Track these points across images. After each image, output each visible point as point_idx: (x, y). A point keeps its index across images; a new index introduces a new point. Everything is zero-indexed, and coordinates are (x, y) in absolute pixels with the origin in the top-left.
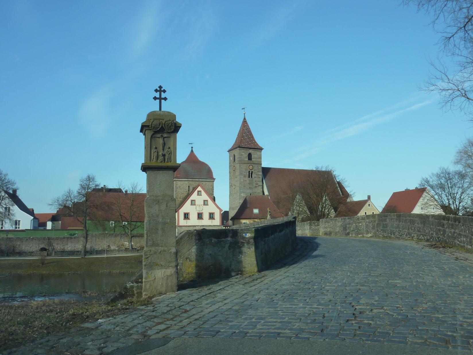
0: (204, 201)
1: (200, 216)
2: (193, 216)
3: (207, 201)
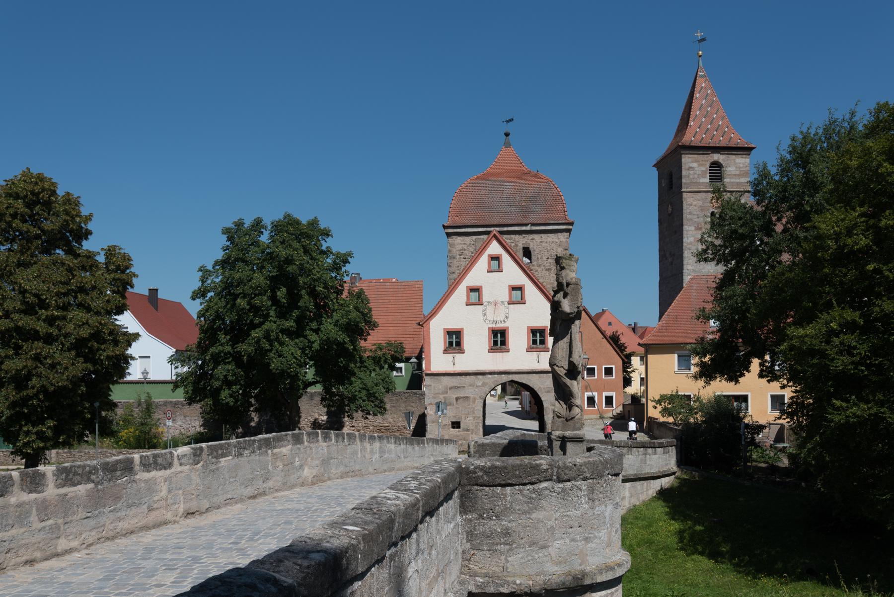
0: (514, 288)
1: (499, 339)
2: (476, 343)
3: (520, 288)
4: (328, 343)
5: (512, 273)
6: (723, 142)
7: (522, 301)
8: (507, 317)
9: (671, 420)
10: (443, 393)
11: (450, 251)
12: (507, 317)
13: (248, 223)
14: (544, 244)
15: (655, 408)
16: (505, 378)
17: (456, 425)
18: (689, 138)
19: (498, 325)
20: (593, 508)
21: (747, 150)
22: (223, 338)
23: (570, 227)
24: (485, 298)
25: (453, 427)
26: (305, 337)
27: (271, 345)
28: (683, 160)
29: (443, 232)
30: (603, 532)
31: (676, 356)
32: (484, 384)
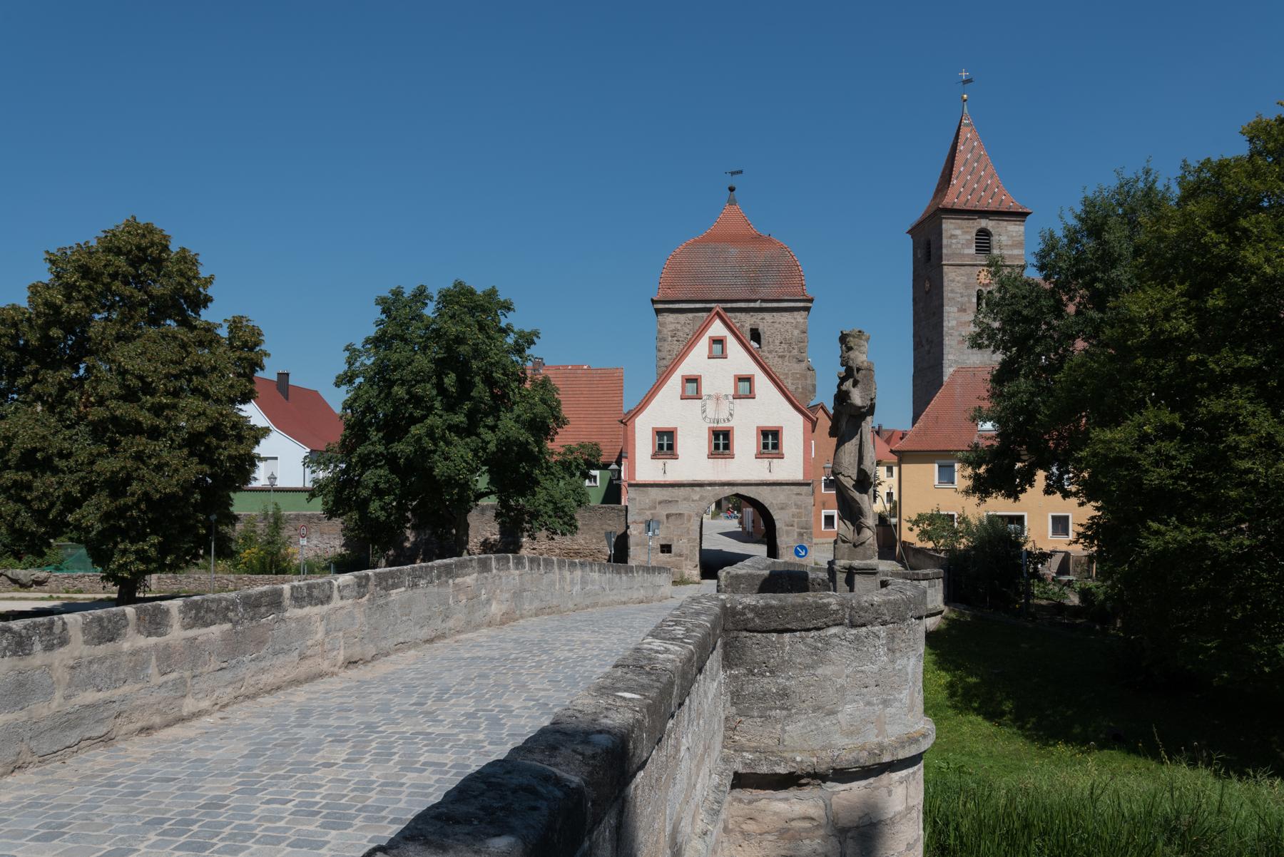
0: (741, 379)
1: (721, 441)
3: (748, 379)
4: (506, 443)
5: (739, 360)
6: (992, 205)
7: (751, 395)
9: (930, 545)
10: (650, 509)
11: (660, 332)
13: (408, 292)
14: (776, 325)
15: (911, 530)
16: (728, 491)
17: (666, 549)
18: (951, 199)
20: (893, 661)
21: (1021, 216)
22: (374, 435)
24: (705, 391)
25: (663, 552)
26: (478, 435)
27: (435, 445)
28: (944, 226)
30: (905, 692)
31: (936, 466)
32: (702, 498)
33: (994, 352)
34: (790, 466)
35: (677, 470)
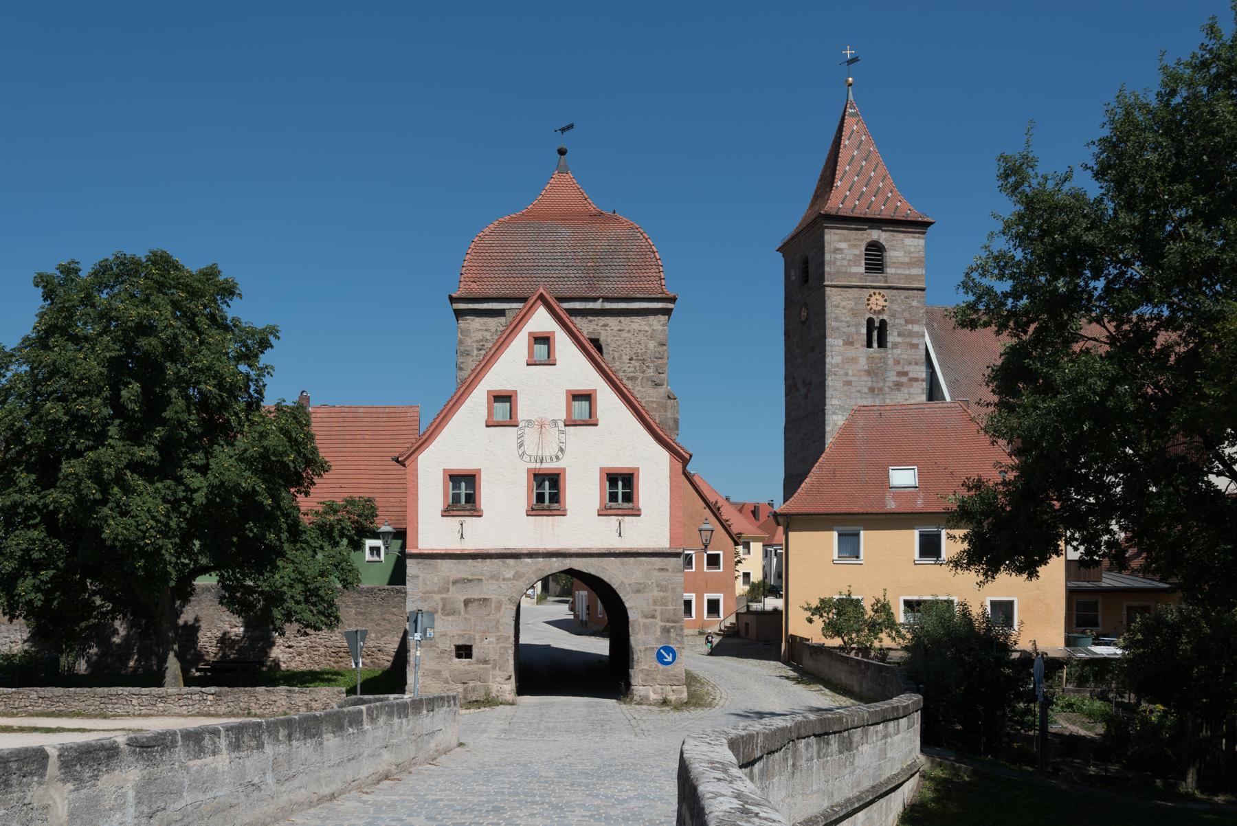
0: (577, 396)
1: (547, 491)
2: (504, 495)
3: (586, 397)
4: (222, 491)
6: (885, 212)
7: (591, 421)
8: (562, 450)
9: (837, 642)
10: (440, 592)
11: (461, 342)
12: (562, 450)
14: (624, 335)
15: (810, 621)
16: (557, 565)
17: (464, 651)
18: (834, 204)
19: (545, 465)
21: (920, 226)
22: (24, 479)
23: (670, 306)
24: (522, 414)
25: (459, 656)
26: (179, 480)
27: (105, 490)
28: (827, 237)
29: (449, 309)
31: (835, 534)
32: (518, 576)
33: (998, 333)
34: (652, 526)
35: (479, 534)
